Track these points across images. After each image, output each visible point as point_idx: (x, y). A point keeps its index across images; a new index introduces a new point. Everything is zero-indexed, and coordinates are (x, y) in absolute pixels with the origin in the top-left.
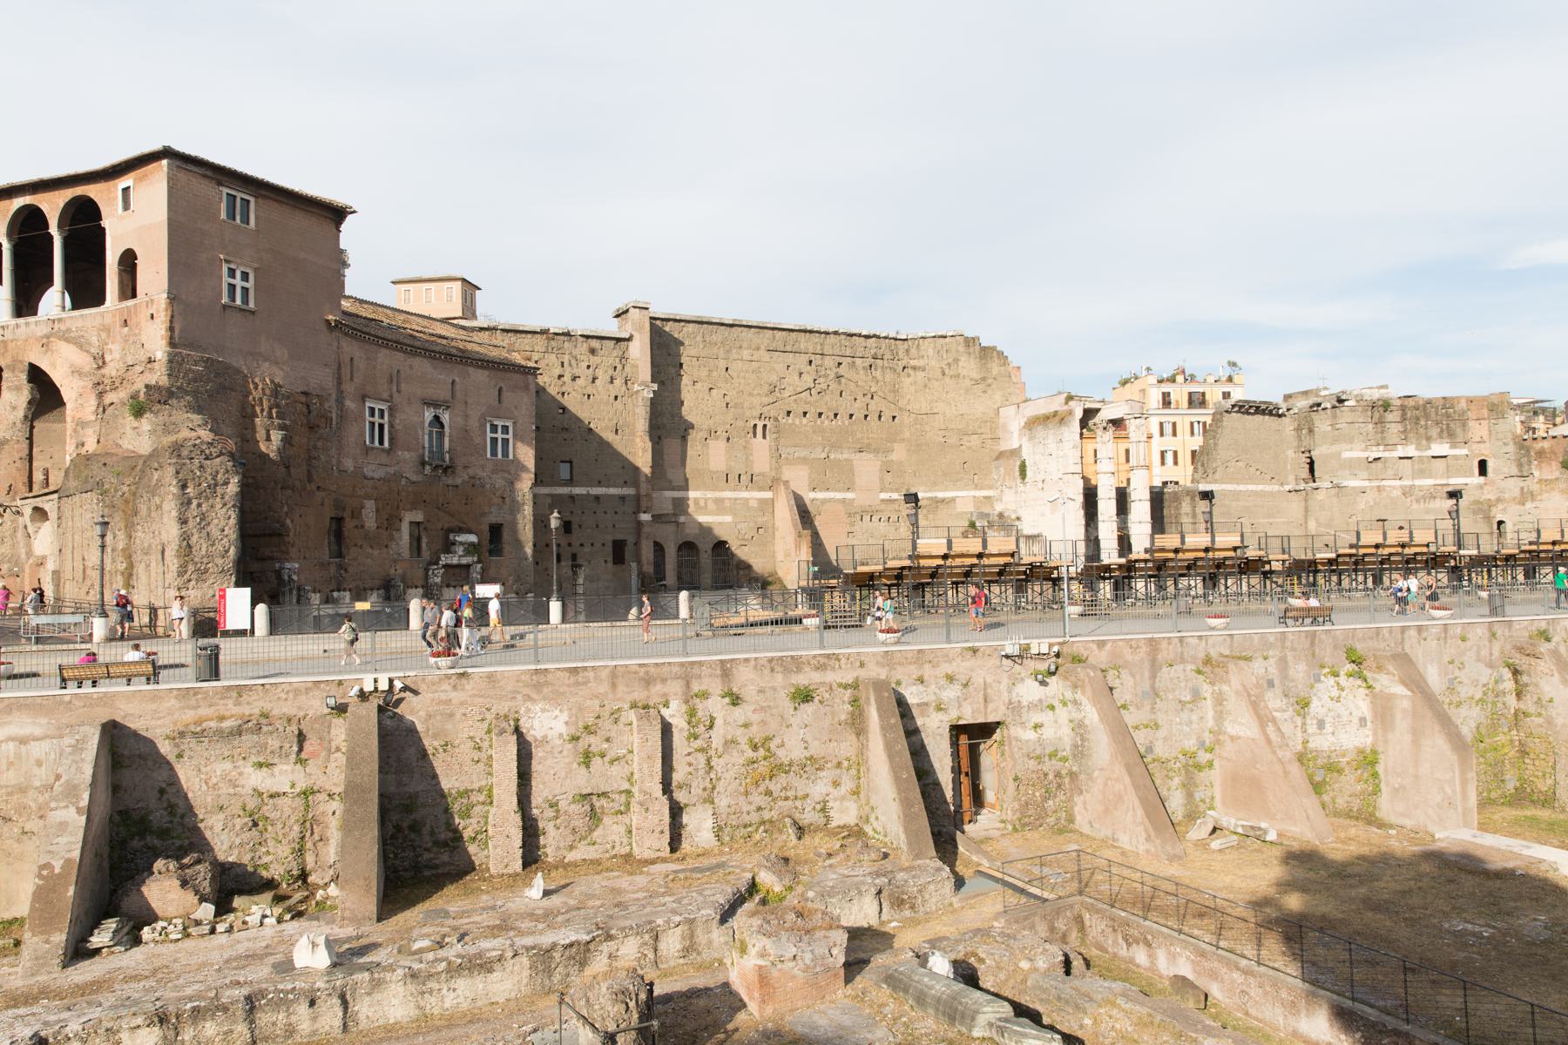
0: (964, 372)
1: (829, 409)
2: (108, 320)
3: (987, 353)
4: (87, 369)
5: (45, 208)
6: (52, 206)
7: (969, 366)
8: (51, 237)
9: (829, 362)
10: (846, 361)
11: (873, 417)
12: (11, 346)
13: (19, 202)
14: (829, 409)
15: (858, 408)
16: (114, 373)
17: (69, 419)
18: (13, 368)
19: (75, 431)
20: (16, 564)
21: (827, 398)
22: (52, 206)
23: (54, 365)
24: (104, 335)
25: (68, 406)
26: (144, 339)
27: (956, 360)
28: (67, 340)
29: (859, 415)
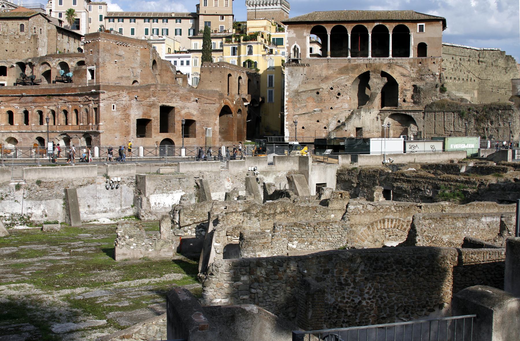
0: (500, 65)
1: (457, 76)
2: (412, 61)
3: (509, 58)
4: (408, 75)
7: (501, 62)
8: (389, 35)
9: (458, 58)
10: (462, 58)
11: (469, 80)
12: (373, 65)
14: (457, 76)
15: (464, 76)
18: (374, 72)
21: (457, 72)
23: (393, 73)
26: (430, 68)
27: (497, 60)
28: (398, 66)
29: (465, 79)
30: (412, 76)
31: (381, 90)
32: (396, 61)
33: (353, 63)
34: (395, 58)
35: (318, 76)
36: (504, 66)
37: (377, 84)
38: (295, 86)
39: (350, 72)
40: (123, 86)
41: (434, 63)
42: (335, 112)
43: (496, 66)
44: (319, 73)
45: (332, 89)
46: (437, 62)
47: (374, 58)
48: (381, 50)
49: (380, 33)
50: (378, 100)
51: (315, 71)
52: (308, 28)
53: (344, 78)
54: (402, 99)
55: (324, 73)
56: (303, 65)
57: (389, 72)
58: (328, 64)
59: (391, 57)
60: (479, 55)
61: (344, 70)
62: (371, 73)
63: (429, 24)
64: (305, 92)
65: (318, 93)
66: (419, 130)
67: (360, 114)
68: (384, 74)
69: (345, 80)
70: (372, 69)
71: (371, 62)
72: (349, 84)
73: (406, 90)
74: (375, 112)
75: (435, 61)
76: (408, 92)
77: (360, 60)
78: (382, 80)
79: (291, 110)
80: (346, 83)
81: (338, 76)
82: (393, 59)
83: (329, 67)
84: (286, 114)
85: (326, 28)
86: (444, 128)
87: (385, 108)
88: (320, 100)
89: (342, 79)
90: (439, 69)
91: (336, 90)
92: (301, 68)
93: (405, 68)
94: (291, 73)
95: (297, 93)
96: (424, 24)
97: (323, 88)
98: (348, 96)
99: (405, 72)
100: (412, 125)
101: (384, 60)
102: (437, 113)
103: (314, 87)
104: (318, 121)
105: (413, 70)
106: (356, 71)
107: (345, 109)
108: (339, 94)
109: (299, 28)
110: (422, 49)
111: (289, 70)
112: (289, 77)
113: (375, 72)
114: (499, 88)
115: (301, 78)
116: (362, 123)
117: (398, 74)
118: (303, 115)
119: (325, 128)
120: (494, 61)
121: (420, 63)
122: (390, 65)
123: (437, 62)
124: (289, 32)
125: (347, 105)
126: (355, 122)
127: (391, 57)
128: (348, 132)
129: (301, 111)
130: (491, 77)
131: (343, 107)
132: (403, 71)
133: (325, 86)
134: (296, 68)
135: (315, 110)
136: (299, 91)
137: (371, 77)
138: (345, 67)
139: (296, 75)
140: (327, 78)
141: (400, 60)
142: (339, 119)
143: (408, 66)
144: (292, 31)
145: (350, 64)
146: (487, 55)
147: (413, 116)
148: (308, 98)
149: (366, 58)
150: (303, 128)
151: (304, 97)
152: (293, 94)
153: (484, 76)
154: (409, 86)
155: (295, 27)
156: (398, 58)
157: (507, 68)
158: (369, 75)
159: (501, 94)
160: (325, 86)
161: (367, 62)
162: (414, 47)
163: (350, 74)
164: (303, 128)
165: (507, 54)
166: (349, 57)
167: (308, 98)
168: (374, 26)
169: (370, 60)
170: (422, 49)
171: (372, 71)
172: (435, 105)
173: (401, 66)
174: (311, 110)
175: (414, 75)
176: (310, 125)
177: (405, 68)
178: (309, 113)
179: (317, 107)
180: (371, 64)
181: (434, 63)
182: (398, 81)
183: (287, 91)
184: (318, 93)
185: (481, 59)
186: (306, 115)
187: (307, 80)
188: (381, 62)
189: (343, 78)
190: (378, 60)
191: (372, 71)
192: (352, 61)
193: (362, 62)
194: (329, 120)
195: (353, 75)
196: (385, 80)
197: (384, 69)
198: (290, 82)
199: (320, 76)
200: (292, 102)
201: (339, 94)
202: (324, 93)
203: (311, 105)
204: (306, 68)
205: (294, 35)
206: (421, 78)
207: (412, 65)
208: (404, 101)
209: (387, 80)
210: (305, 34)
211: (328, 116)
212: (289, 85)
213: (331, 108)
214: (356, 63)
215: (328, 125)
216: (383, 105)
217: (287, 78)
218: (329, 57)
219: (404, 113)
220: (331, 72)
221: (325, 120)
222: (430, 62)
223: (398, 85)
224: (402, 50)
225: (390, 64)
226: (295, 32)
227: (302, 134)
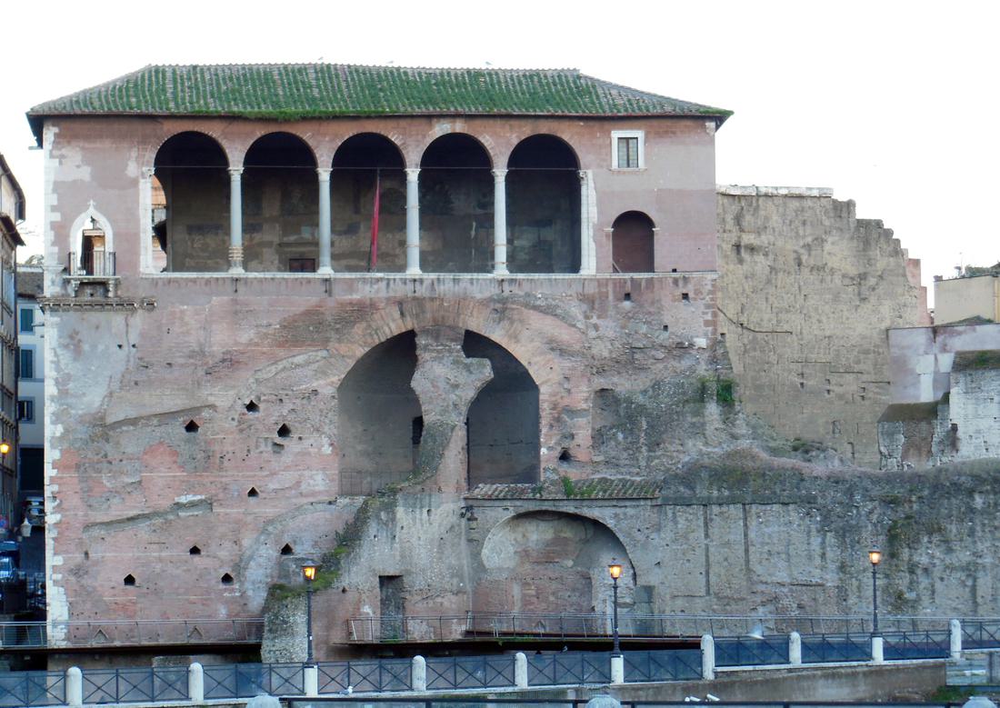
0: (833, 262)
2: (591, 289)
4: (577, 347)
5: (487, 141)
6: (500, 144)
7: (839, 253)
12: (428, 305)
13: (441, 129)
16: (606, 354)
17: (545, 407)
18: (436, 332)
19: (558, 420)
20: (462, 580)
22: (500, 144)
23: (515, 338)
24: (585, 307)
25: (545, 392)
26: (667, 320)
27: (820, 241)
28: (535, 308)
30: (595, 351)
31: (464, 410)
32: (526, 287)
33: (342, 296)
34: (520, 276)
35: (192, 355)
36: (853, 271)
37: (445, 383)
38: (93, 399)
39: (333, 335)
40: (586, 518)
41: (685, 296)
42: (269, 511)
43: (818, 268)
44: (193, 340)
45: (252, 407)
46: (698, 292)
47: (433, 276)
48: (459, 244)
49: (456, 163)
50: (453, 460)
51: (176, 329)
52: (144, 141)
53: (308, 363)
54: (557, 453)
55: (221, 339)
56: (126, 305)
57: (497, 335)
58: (235, 302)
59: (501, 271)
60: (738, 219)
61: (306, 330)
62: (421, 341)
63: (659, 135)
64: (133, 422)
65: (192, 427)
66: (641, 582)
67: (393, 520)
68: (475, 344)
69: (308, 371)
70: (429, 325)
71: (422, 291)
72: (328, 385)
73: (572, 412)
74: (446, 507)
75: (690, 289)
76: (581, 421)
77: (373, 285)
78: (467, 368)
79: (74, 501)
80: (315, 385)
81: (281, 352)
82: (512, 281)
83: (237, 314)
84: (51, 519)
85: (225, 144)
86: (749, 570)
87: (483, 489)
88: (200, 456)
89: (298, 366)
90: (707, 323)
91: (270, 416)
92: (118, 319)
93: (565, 319)
94: (73, 342)
95: (102, 429)
96: (640, 134)
97: (213, 407)
98: (325, 441)
99: (564, 334)
100: (606, 557)
101: (476, 285)
102: (716, 509)
103: (173, 401)
104: (195, 551)
105: (596, 327)
106: (359, 329)
107: (313, 494)
108: (284, 431)
109: (106, 144)
110: (634, 231)
111: (61, 327)
112: (66, 357)
113: (437, 338)
114: (831, 369)
115: (119, 361)
116: (403, 556)
117: (537, 344)
118: (129, 530)
119: (227, 579)
120: (808, 247)
121: (628, 296)
122: (501, 308)
123: (698, 292)
124: (62, 157)
125: (319, 477)
126: (376, 555)
127: (501, 271)
128: (351, 596)
129: (118, 510)
130: (794, 321)
131: (303, 487)
132: (555, 325)
133: (224, 397)
134: (95, 317)
135: (183, 500)
136: (110, 420)
137: (423, 356)
138: (308, 313)
139: (94, 347)
140: (231, 362)
141: (543, 284)
142: (286, 540)
143: (576, 310)
144: (74, 154)
145: (331, 302)
146: (775, 220)
147: (610, 523)
148: (150, 451)
149: (398, 276)
150: (130, 580)
151: (131, 443)
152: (82, 432)
153: (762, 316)
154: (582, 395)
155: (87, 138)
156: (536, 276)
157: (863, 277)
158: (413, 346)
159: (841, 397)
160: (224, 397)
161: (400, 291)
162: (598, 229)
163: (333, 345)
164: (130, 580)
165: (862, 213)
166: (325, 271)
167: (150, 451)
168: (429, 141)
169: (409, 278)
170: (634, 231)
171: (426, 332)
172: (704, 474)
173: (548, 311)
174: (165, 504)
175: (602, 350)
176: (158, 567)
177: (565, 319)
178: (156, 514)
179: (191, 489)
180: (419, 301)
181: (685, 296)
182: (537, 374)
183: (57, 418)
184: (192, 427)
185: (748, 239)
186: (143, 526)
187: (143, 369)
188: (474, 292)
189: (299, 359)
190: (449, 284)
191: (426, 332)
192: (336, 289)
193: (383, 294)
194: (246, 542)
195: (343, 348)
196: (484, 371)
197: (479, 323)
198: (68, 377)
199: (200, 353)
200: (78, 467)
201: (284, 431)
202: (221, 428)
203: (165, 482)
204: (139, 320)
205: (85, 173)
206: (632, 361)
207: (592, 302)
208: (565, 457)
209: (494, 368)
210: (132, 169)
211: (238, 526)
212: (63, 393)
213: (253, 493)
214: (356, 297)
215: (240, 566)
216: (471, 481)
217: (57, 363)
218: (238, 271)
219: (570, 508)
220: (246, 335)
221: (228, 544)
222: (667, 296)
223: (532, 387)
224: (549, 240)
225: (504, 301)
226: (86, 161)
227: (124, 607)
